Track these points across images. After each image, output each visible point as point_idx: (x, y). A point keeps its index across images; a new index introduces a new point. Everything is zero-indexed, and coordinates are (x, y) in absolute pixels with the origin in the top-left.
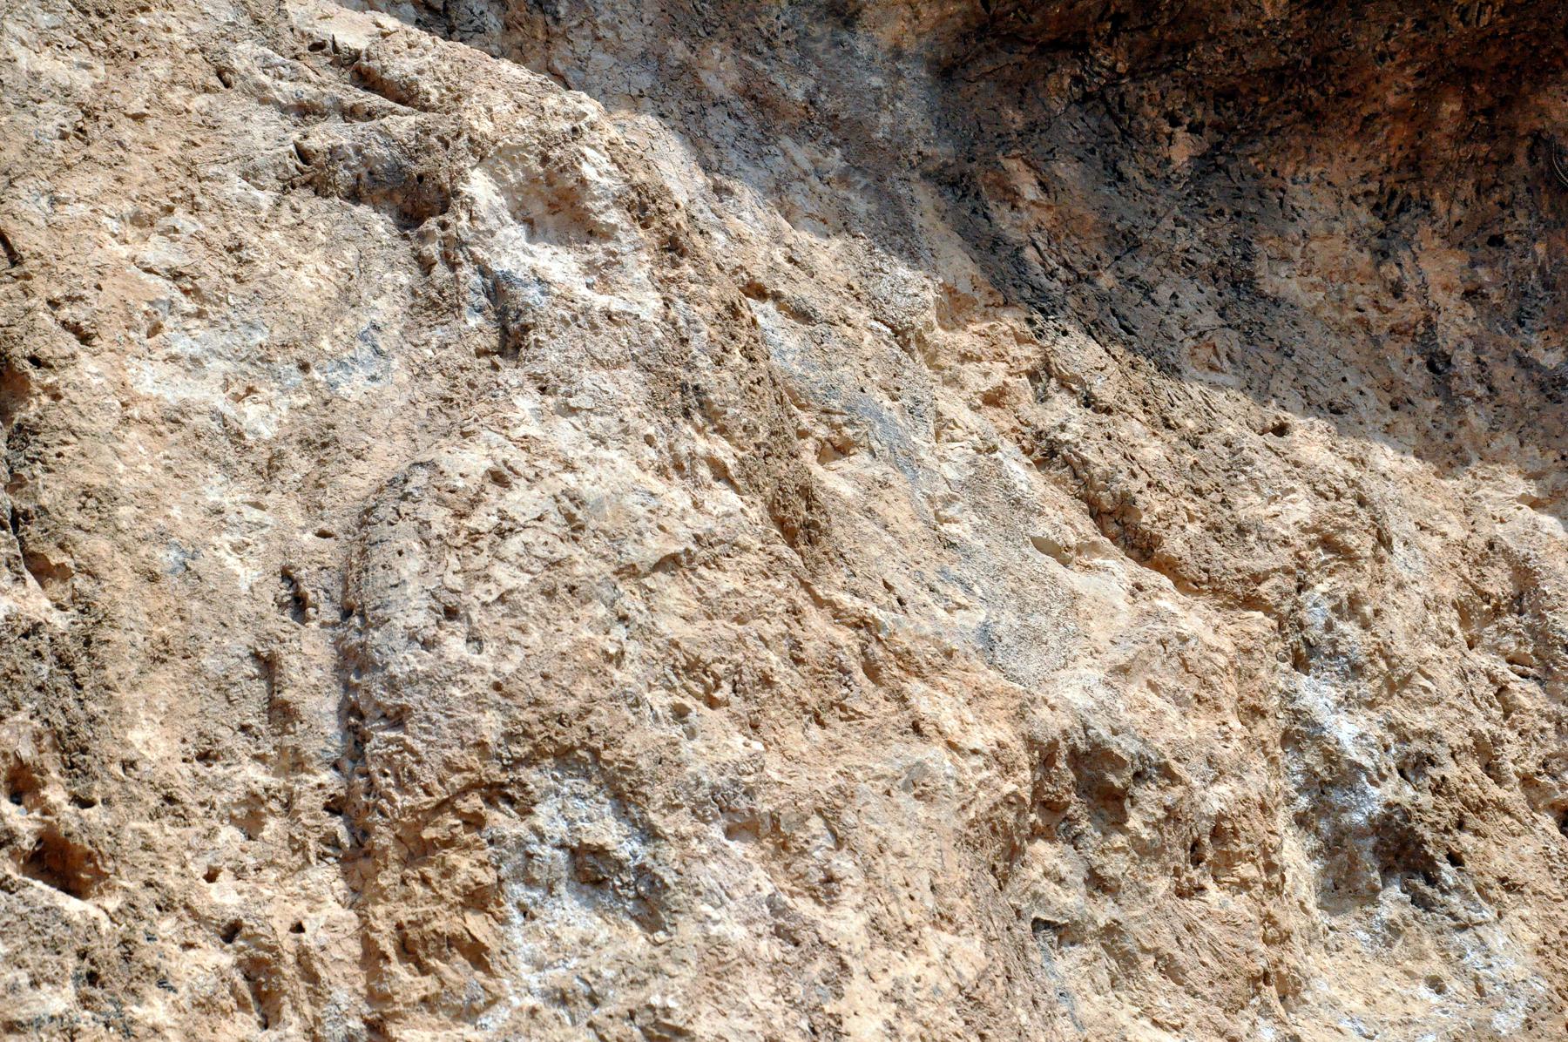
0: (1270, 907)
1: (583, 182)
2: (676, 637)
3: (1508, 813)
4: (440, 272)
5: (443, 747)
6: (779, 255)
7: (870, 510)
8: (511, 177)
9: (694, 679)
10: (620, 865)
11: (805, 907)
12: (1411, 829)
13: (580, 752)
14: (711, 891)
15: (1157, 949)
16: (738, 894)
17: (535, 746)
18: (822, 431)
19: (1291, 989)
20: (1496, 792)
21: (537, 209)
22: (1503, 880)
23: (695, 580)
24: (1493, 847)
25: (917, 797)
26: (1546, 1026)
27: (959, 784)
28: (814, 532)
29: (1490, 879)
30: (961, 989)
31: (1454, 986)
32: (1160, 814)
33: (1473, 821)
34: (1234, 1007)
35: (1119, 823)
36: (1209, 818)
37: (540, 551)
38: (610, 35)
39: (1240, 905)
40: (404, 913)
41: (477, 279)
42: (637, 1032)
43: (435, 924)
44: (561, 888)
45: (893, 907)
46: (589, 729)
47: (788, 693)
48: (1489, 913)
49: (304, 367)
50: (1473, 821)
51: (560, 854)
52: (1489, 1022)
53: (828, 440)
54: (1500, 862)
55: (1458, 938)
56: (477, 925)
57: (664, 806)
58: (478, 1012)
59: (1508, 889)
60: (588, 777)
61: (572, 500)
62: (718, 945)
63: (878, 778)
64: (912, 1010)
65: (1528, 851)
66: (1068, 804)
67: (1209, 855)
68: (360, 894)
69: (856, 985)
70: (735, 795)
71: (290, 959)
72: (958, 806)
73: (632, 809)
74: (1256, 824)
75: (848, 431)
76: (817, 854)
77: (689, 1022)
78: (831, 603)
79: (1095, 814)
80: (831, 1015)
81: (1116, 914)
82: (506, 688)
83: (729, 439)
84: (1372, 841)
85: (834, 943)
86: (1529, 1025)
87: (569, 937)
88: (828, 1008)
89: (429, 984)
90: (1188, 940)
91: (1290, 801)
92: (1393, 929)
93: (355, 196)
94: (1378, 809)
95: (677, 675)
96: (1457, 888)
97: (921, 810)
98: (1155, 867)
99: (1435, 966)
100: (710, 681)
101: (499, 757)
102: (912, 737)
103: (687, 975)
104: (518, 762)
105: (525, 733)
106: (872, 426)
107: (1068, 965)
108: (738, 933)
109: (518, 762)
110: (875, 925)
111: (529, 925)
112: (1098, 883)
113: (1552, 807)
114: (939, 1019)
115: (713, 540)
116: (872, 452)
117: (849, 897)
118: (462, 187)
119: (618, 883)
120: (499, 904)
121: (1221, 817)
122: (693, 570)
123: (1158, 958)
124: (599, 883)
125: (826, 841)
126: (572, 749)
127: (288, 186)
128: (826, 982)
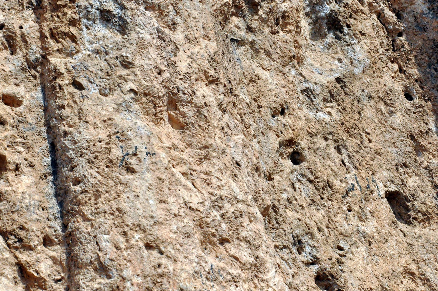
0: (297, 38)
3: (364, 13)
10: (114, 16)
11: (167, 31)
12: (337, 18)
14: (140, 25)
15: (265, 48)
16: (148, 26)
19: (300, 61)
20: (361, 7)
22: (360, 32)
24: (359, 23)
26: (368, 72)
29: (357, 32)
30: (210, 56)
31: (345, 61)
32: (268, 10)
33: (354, 15)
34: (285, 65)
35: (256, 12)
36: (281, 12)
39: (288, 37)
40: (52, 25)
42: (118, 63)
43: (61, 29)
44: (98, 21)
45: (192, 32)
48: (356, 41)
50: (354, 15)
51: (97, 11)
52: (353, 70)
54: (360, 27)
55: (347, 48)
56: (73, 30)
58: (73, 55)
59: (362, 35)
62: (142, 40)
64: (196, 61)
65: (368, 24)
66: (242, 6)
67: (281, 23)
68: (39, 19)
69: (181, 54)
71: (19, 36)
72: (211, 5)
74: (294, 14)
76: (171, 16)
77: (133, 60)
79: (250, 9)
80: (173, 61)
81: (254, 38)
84: (326, 21)
85: (175, 41)
86: (364, 71)
87: (100, 35)
88: (172, 59)
89: (59, 46)
90: (273, 46)
91: (304, 9)
92: (330, 45)
94: (328, 12)
96: (348, 34)
98: (266, 25)
99: (340, 55)
103: (133, 48)
107: (240, 51)
108: (148, 37)
110: (186, 37)
111: (88, 31)
112: (250, 29)
113: (376, 12)
114: (203, 64)
117: (180, 29)
120: (80, 25)
121: (285, 12)
123: (265, 51)
124: (108, 21)
125: (174, 13)
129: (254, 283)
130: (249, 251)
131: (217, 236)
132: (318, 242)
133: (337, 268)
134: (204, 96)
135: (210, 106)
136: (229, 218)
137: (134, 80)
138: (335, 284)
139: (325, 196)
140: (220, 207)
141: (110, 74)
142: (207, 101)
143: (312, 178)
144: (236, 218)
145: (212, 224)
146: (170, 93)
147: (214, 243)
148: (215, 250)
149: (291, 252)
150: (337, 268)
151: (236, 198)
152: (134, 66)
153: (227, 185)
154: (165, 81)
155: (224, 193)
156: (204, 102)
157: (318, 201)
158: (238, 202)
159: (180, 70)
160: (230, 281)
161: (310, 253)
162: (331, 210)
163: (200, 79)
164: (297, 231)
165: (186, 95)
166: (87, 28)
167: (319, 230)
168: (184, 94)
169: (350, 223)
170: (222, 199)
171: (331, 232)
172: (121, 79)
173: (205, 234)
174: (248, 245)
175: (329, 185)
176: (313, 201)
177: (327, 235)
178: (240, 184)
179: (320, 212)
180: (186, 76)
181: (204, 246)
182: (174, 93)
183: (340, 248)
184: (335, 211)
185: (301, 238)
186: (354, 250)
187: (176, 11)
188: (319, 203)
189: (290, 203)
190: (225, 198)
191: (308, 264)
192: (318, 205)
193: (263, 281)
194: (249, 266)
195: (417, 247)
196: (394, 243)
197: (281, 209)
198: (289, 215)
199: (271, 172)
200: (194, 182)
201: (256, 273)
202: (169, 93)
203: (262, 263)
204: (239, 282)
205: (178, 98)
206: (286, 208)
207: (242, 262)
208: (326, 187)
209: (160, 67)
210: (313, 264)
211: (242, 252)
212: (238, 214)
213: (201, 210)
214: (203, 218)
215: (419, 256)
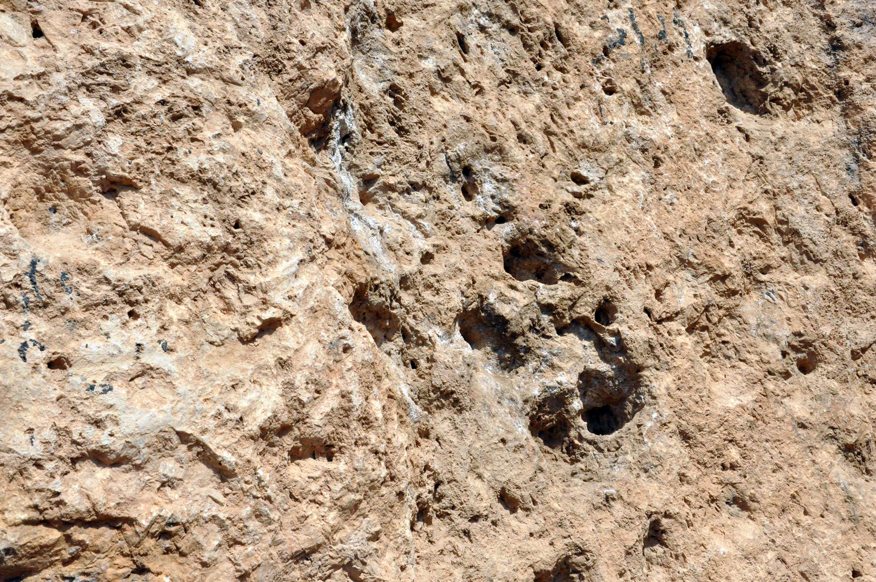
129: (223, 298)
130: (210, 209)
131: (92, 172)
132: (515, 168)
133: (565, 225)
136: (144, 118)
138: (557, 263)
139: (547, 62)
140: (115, 89)
143: (516, 21)
144: (176, 118)
145: (75, 138)
147: (83, 194)
148: (86, 214)
149: (437, 198)
150: (565, 225)
151: (180, 61)
153: (156, 26)
155: (135, 49)
157: (525, 74)
158: (190, 72)
160: (107, 303)
161: (493, 197)
162: (559, 93)
164: (460, 147)
167: (522, 139)
169: (609, 119)
170: (128, 66)
171: (557, 144)
173: (50, 168)
174: (209, 190)
175: (560, 35)
176: (515, 74)
177: (543, 151)
178: (211, 23)
179: (531, 98)
181: (50, 204)
183: (579, 179)
184: (571, 93)
185: (471, 161)
186: (613, 180)
188: (528, 78)
189: (447, 80)
190: (139, 62)
191: (486, 222)
192: (526, 82)
193: (249, 290)
194: (197, 253)
195: (776, 162)
196: (719, 159)
197: (415, 96)
198: (440, 109)
199: (392, 8)
200: (39, 18)
201: (232, 270)
203: (254, 238)
204: (146, 301)
206: (434, 93)
207: (170, 241)
208: (551, 40)
210: (501, 220)
211: (175, 214)
212: (182, 105)
213: (30, 98)
214: (37, 120)
215: (779, 180)
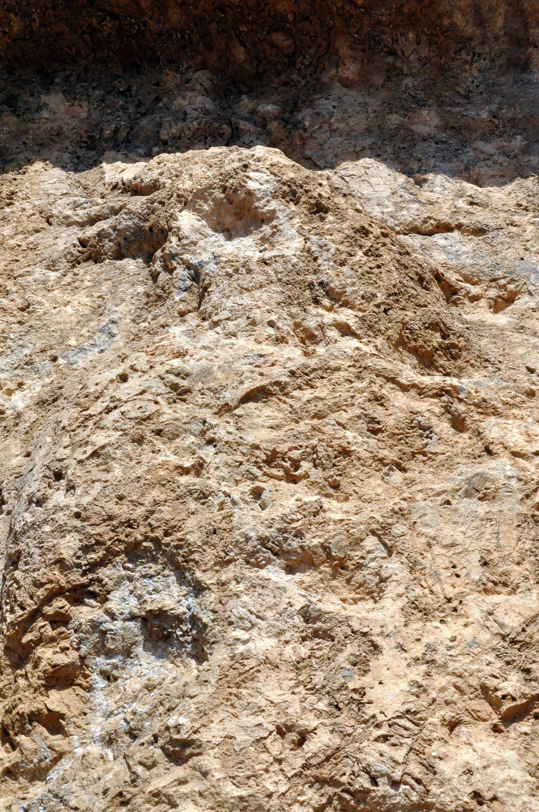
1: (250, 193)
2: (257, 442)
4: (163, 277)
5: (34, 571)
6: (461, 203)
7: (522, 327)
8: (206, 207)
9: (275, 467)
10: (179, 619)
13: (145, 544)
14: (241, 618)
16: (269, 614)
17: (107, 550)
18: (493, 293)
21: (228, 220)
23: (287, 400)
25: (481, 499)
27: (520, 480)
28: (454, 351)
30: (504, 637)
37: (133, 414)
38: (342, 126)
41: (186, 273)
42: (159, 751)
44: (139, 650)
45: (436, 588)
46: (150, 525)
47: (365, 455)
49: (54, 359)
51: (131, 624)
53: (500, 297)
57: (215, 564)
58: (47, 770)
60: (155, 560)
61: (177, 375)
63: (438, 494)
64: (445, 666)
70: (286, 539)
72: (520, 496)
73: (187, 574)
75: (511, 287)
76: (373, 564)
77: (195, 732)
78: (414, 386)
80: (355, 690)
82: (83, 514)
83: (352, 308)
85: (365, 630)
88: (351, 686)
93: (119, 256)
95: (260, 468)
97: (483, 508)
100: (288, 464)
101: (79, 566)
102: (486, 458)
104: (94, 566)
105: (98, 543)
106: (528, 278)
109: (94, 566)
111: (113, 685)
114: (475, 667)
115: (307, 371)
116: (530, 294)
118: (174, 224)
119: (179, 633)
120: (86, 676)
122: (286, 395)
124: (168, 638)
126: (138, 543)
127: (75, 262)
128: (354, 665)
134: (470, 772)
135: (495, 798)
137: (201, 794)
141: (129, 796)
142: (481, 786)
146: (347, 797)
152: (200, 746)
154: (314, 762)
156: (469, 790)
159: (377, 712)
163: (467, 718)
165: (403, 787)
166: (108, 679)
168: (395, 784)
172: (157, 803)
180: (403, 722)
182: (358, 791)
187: (385, 545)
202: (340, 799)
205: (378, 803)
209: (300, 722)
